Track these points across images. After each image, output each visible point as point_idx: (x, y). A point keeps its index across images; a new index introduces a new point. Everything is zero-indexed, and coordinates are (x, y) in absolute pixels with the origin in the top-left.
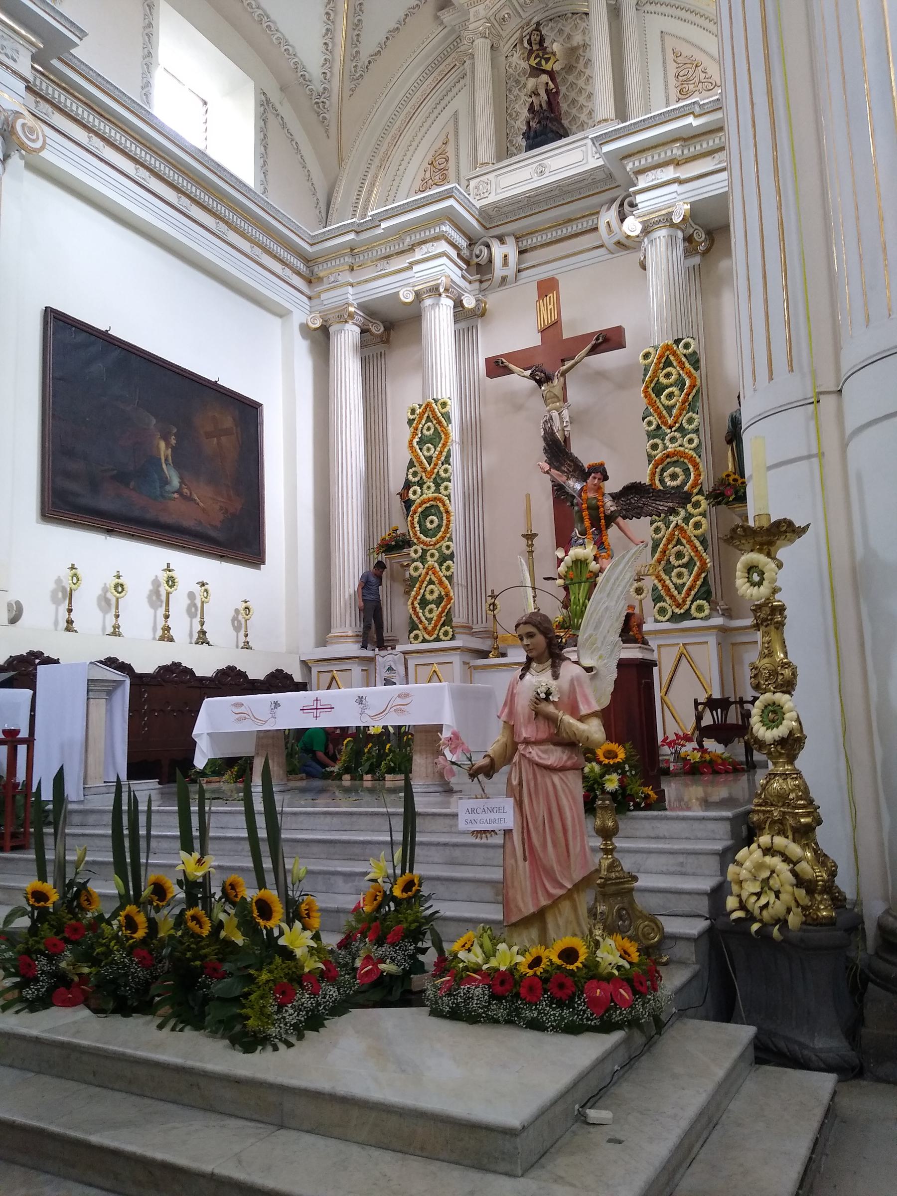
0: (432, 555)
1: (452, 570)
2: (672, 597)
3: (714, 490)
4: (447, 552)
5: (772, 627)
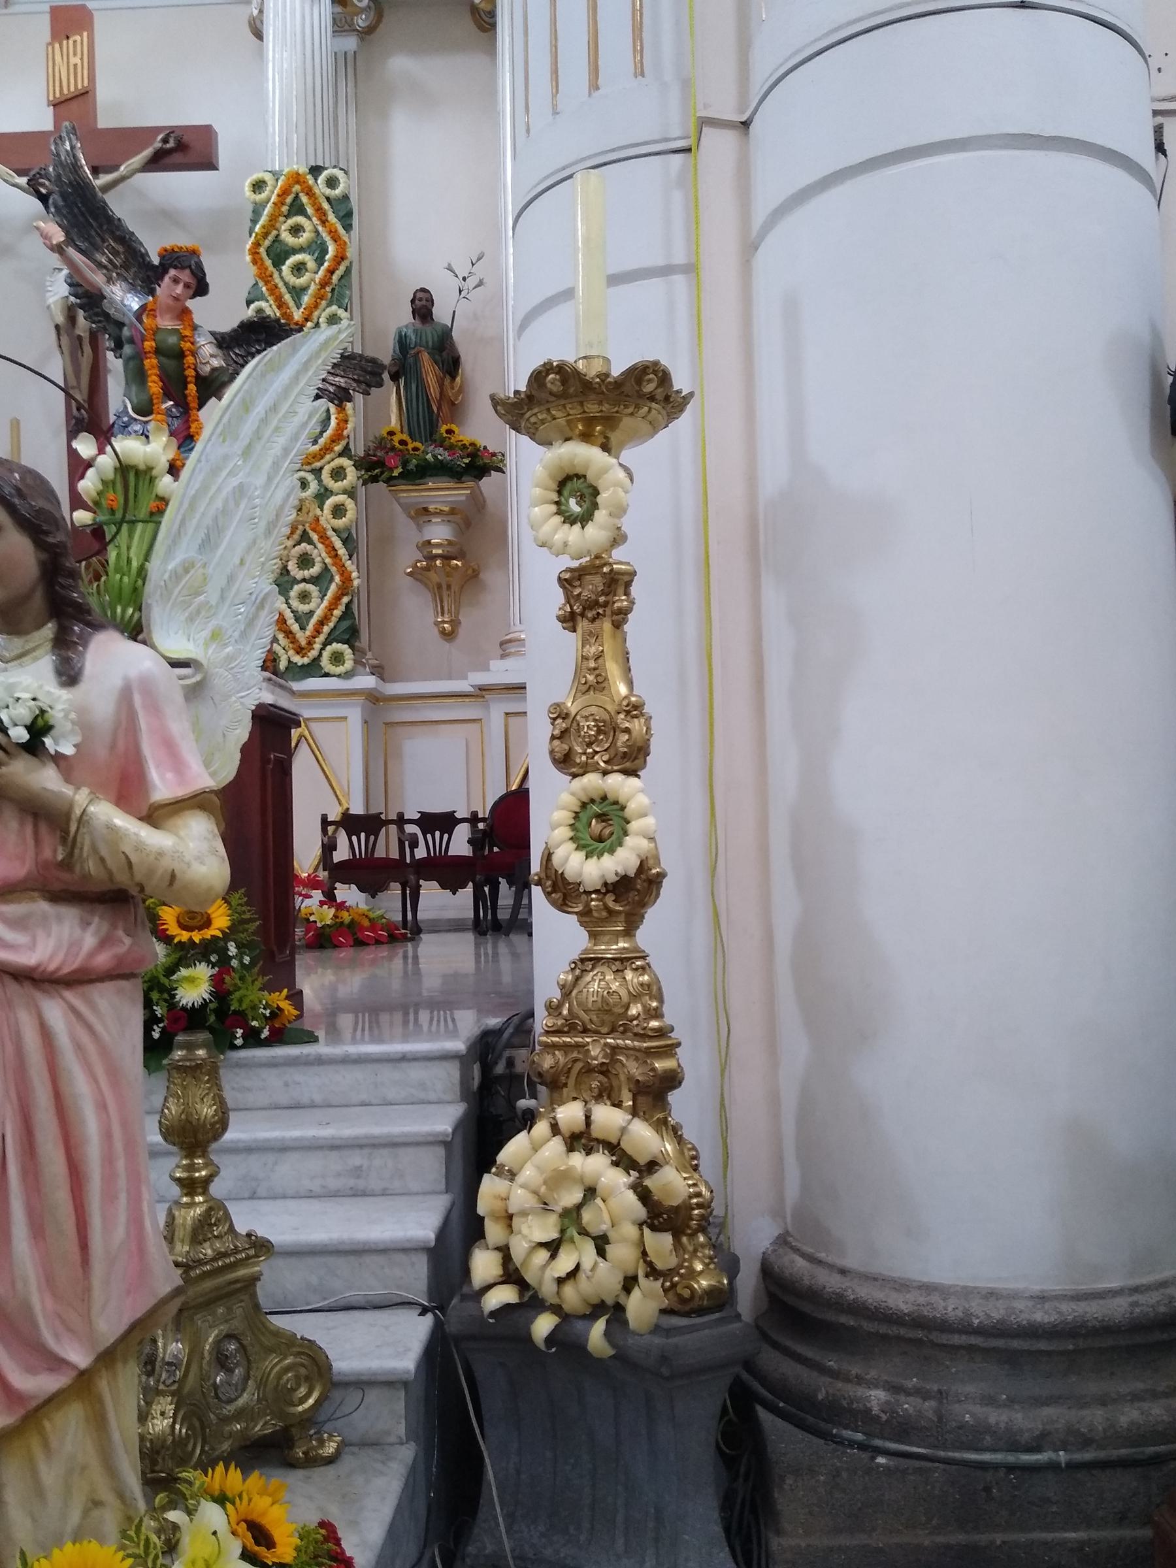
3: (367, 454)
5: (607, 625)
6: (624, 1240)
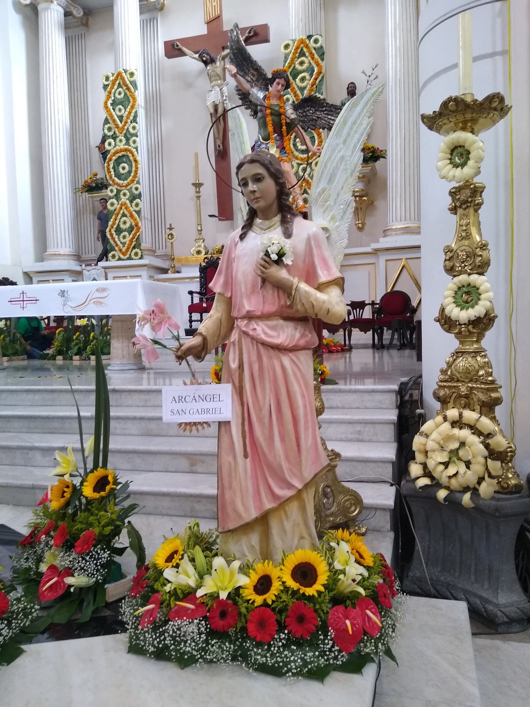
0: (125, 194)
1: (140, 206)
4: (137, 193)
5: (471, 211)
6: (478, 463)
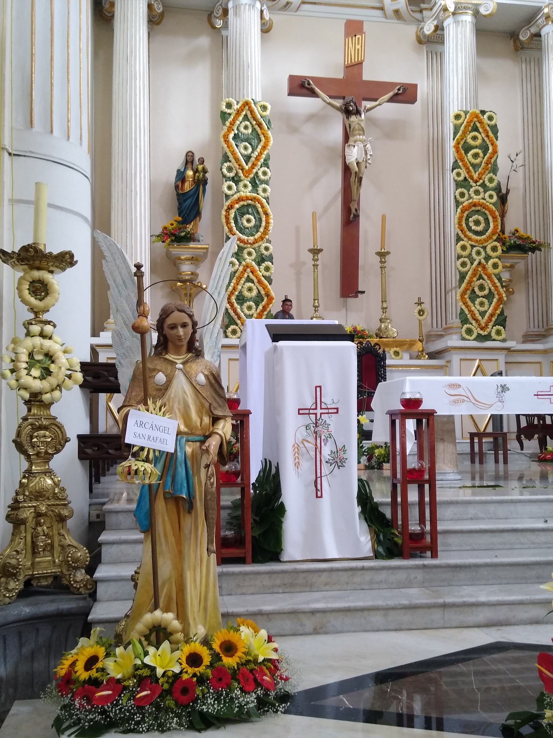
2: (477, 320)
